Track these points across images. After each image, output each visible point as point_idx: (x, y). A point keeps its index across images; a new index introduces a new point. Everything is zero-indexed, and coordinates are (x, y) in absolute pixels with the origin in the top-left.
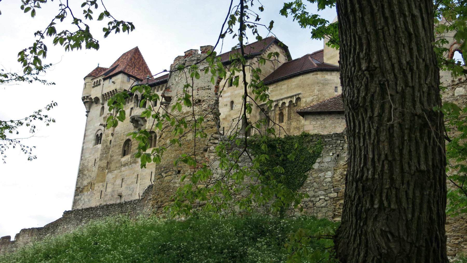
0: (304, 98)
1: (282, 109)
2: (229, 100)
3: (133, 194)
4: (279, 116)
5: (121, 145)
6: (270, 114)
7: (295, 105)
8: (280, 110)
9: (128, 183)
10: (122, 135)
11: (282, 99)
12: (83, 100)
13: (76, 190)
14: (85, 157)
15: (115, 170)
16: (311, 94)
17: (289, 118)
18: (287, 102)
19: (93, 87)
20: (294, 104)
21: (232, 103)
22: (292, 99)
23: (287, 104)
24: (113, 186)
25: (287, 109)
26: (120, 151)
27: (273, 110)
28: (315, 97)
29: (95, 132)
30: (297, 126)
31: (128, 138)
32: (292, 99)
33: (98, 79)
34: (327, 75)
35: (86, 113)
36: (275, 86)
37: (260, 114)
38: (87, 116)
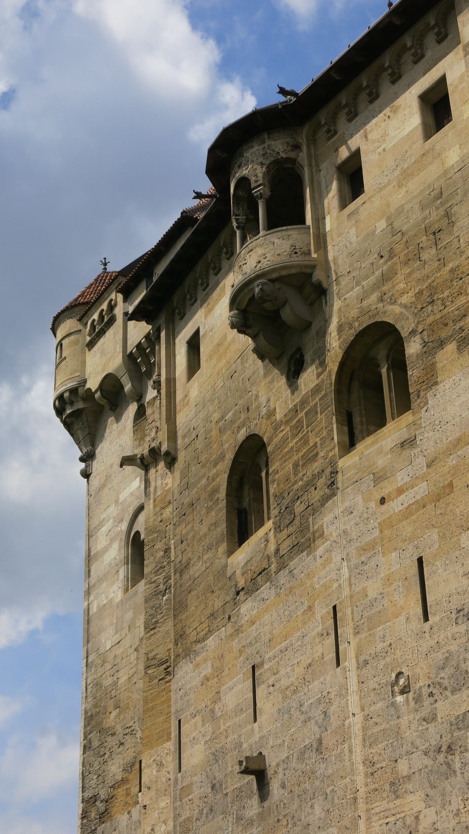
3: (329, 741)
5: (216, 490)
9: (284, 683)
10: (214, 433)
12: (59, 412)
13: (84, 815)
14: (102, 650)
15: (210, 632)
19: (91, 345)
24: (209, 728)
26: (215, 524)
29: (124, 526)
31: (242, 435)
33: (104, 306)
35: (83, 465)
38: (86, 474)
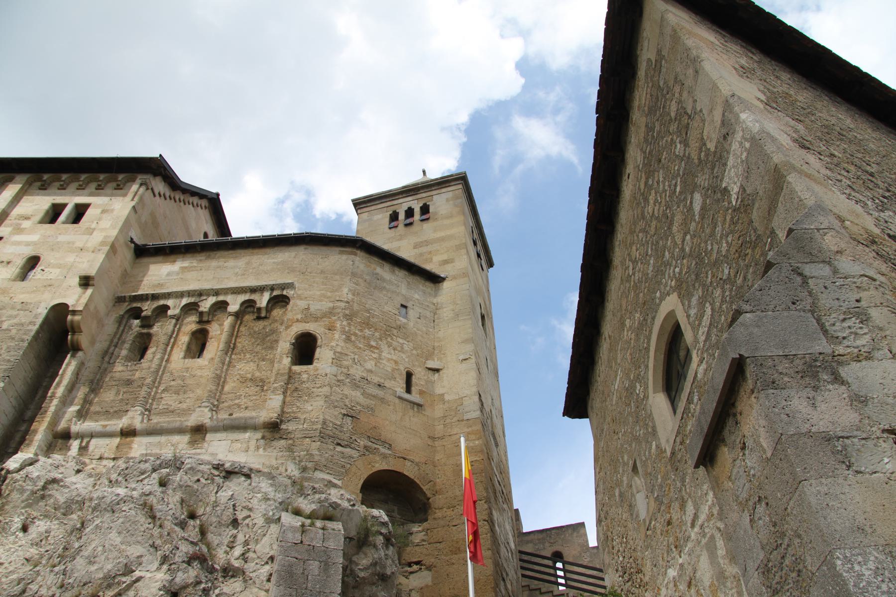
0: (300, 298)
1: (208, 322)
2: (29, 252)
4: (191, 339)
6: (155, 329)
7: (263, 315)
8: (200, 322)
11: (217, 293)
16: (329, 294)
17: (230, 347)
18: (235, 304)
20: (259, 309)
21: (33, 262)
22: (254, 297)
23: (234, 307)
25: (228, 321)
27: (172, 317)
28: (343, 305)
30: (257, 374)
32: (254, 297)
34: (382, 267)
36: (202, 256)
37: (120, 320)
